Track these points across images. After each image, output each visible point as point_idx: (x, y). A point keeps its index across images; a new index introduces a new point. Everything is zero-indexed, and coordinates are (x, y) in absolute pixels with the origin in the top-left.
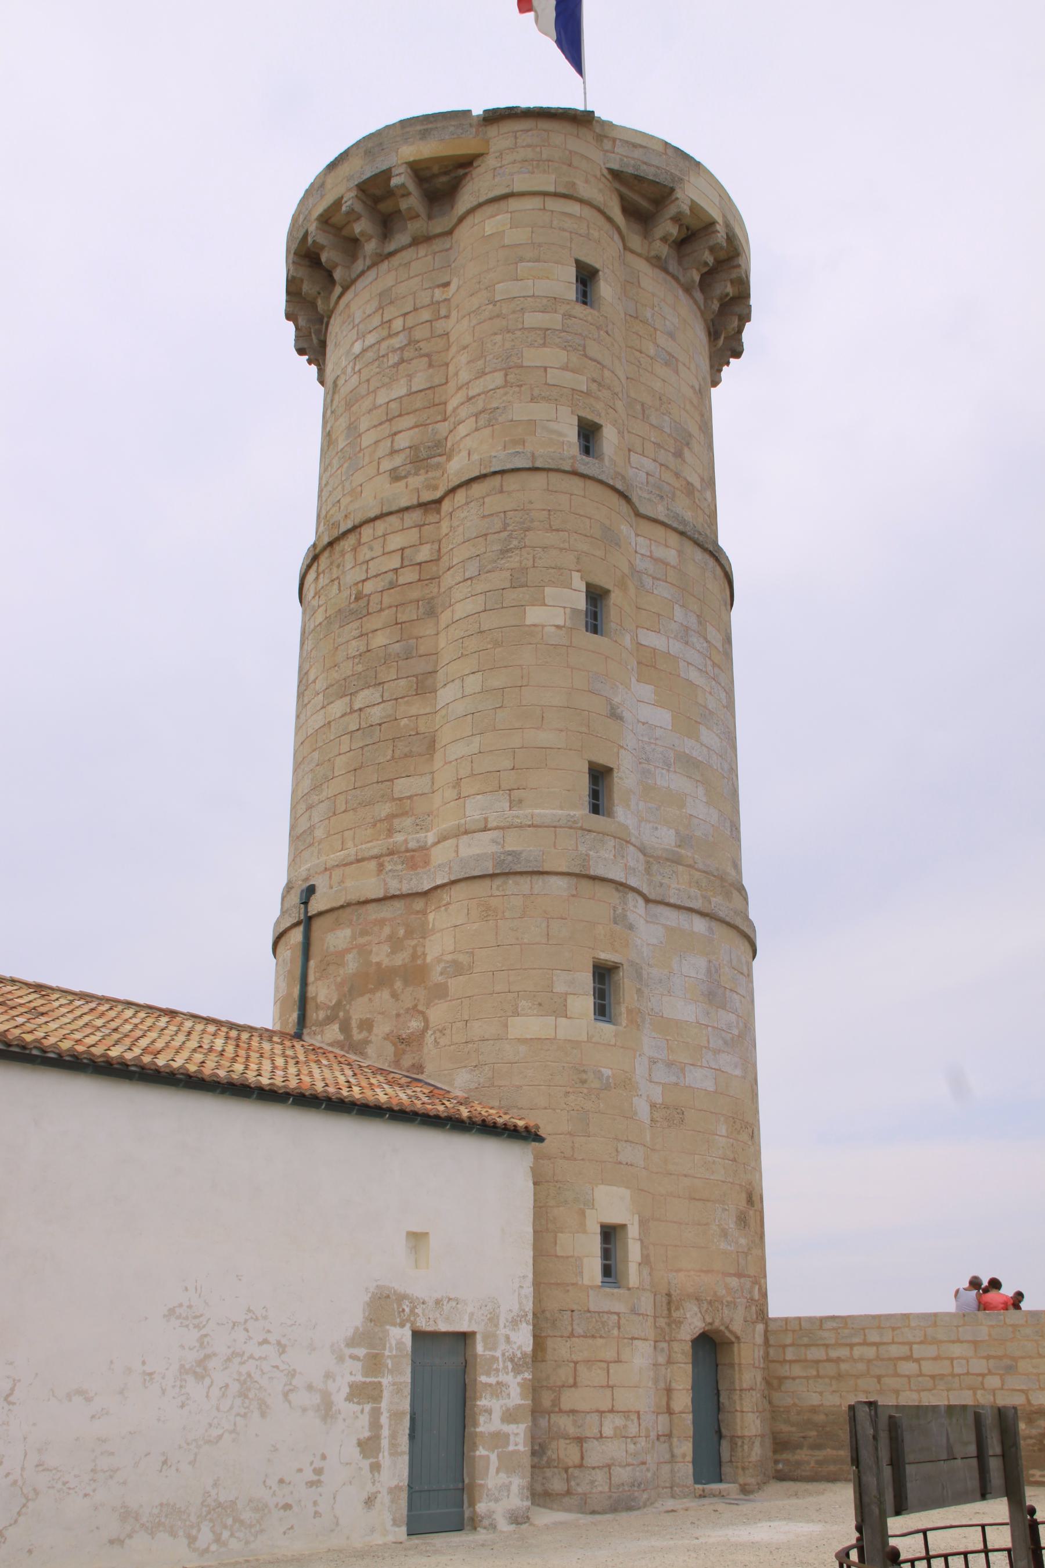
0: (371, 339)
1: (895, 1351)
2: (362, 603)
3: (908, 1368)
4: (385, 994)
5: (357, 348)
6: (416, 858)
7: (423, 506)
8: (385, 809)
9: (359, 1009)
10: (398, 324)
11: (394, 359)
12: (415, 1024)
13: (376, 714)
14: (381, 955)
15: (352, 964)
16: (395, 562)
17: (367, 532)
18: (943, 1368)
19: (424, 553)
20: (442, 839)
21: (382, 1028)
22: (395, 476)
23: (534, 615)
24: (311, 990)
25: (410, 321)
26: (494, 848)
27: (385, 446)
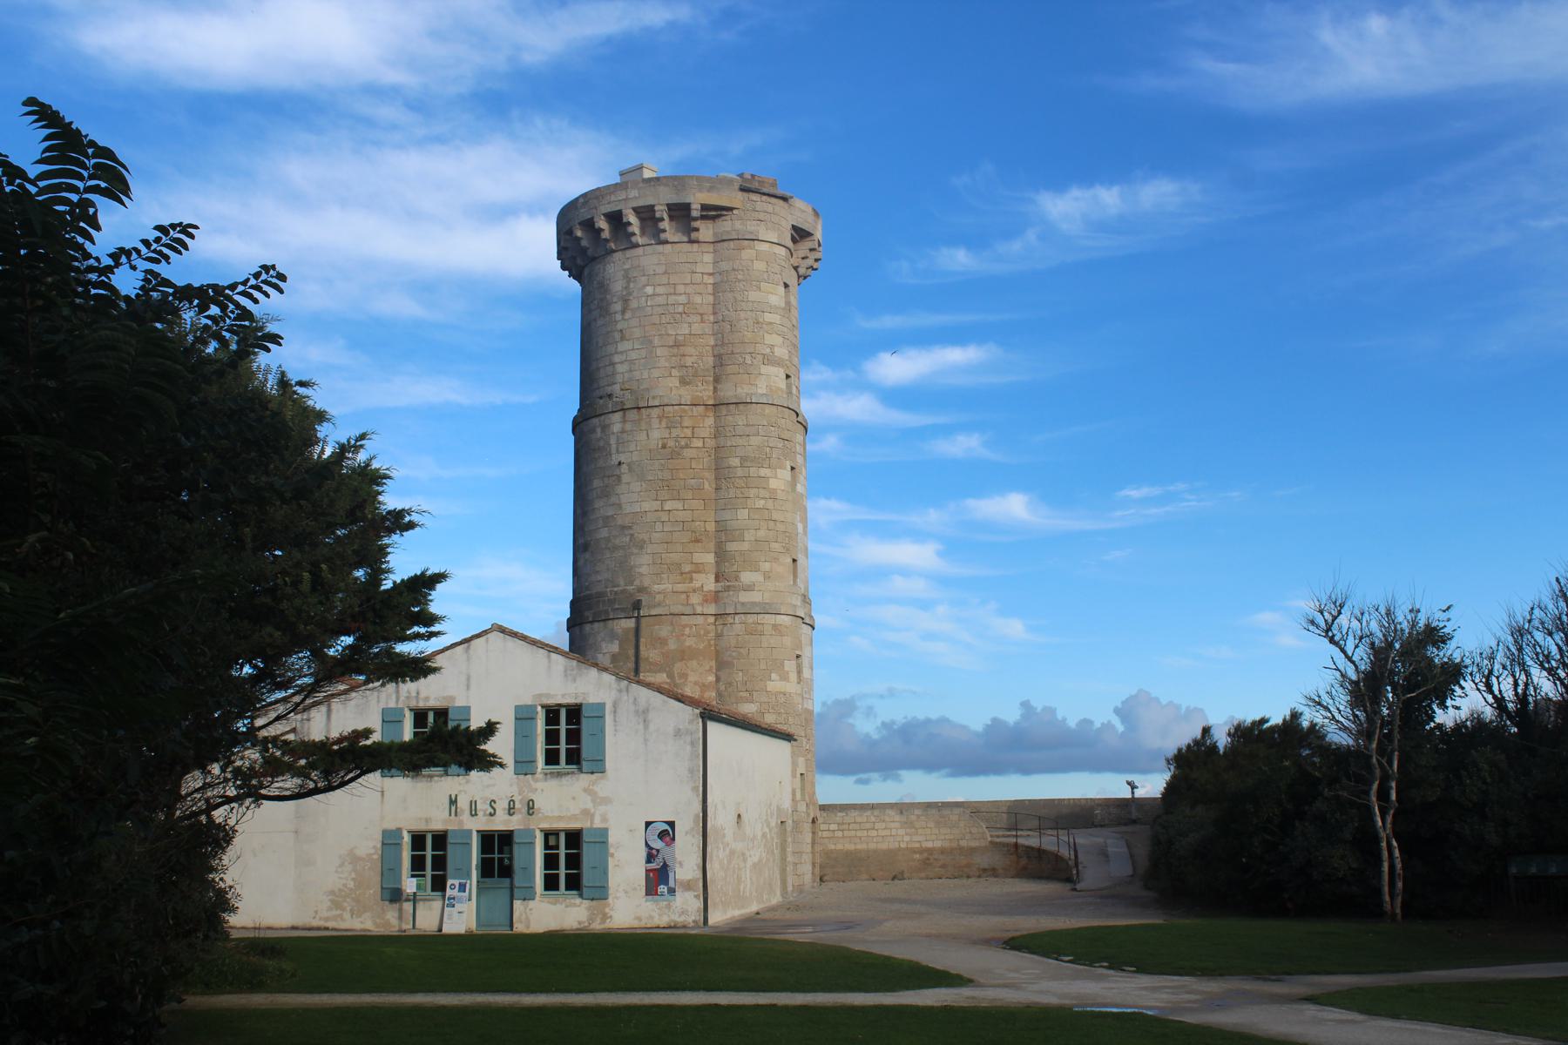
1: (868, 826)
2: (668, 451)
3: (874, 833)
4: (694, 663)
5: (649, 290)
8: (687, 568)
9: (678, 667)
10: (681, 289)
13: (681, 515)
18: (887, 832)
21: (692, 678)
23: (773, 484)
25: (689, 290)
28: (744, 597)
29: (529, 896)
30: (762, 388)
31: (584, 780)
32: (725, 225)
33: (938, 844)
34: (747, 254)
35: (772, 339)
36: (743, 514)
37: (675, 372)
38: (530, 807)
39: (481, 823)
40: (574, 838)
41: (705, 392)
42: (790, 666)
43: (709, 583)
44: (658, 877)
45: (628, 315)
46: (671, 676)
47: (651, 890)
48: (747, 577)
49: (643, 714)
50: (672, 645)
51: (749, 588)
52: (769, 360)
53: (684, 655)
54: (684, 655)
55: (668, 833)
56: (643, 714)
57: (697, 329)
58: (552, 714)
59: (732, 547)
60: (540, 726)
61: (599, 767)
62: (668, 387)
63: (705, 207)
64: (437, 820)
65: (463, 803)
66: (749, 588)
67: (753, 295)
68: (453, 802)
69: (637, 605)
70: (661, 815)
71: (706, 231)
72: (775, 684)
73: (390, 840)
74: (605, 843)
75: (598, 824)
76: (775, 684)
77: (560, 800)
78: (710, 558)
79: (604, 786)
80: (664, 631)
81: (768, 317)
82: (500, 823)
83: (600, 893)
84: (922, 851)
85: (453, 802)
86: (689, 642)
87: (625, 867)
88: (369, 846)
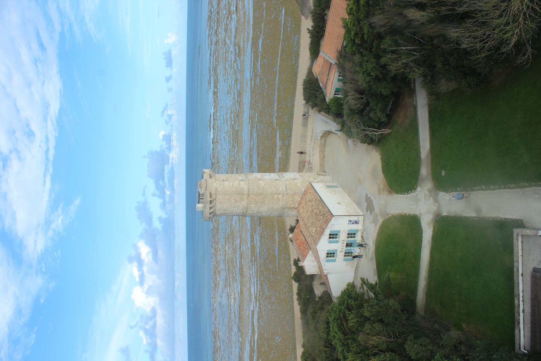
23: (263, 184)
28: (284, 190)
29: (356, 240)
30: (245, 187)
31: (341, 233)
32: (213, 193)
34: (219, 189)
35: (235, 184)
36: (269, 190)
38: (343, 241)
39: (345, 248)
40: (348, 234)
41: (245, 197)
42: (296, 181)
43: (281, 196)
44: (356, 222)
47: (358, 223)
48: (280, 190)
49: (332, 225)
50: (291, 202)
51: (282, 189)
52: (240, 185)
53: (293, 200)
54: (293, 200)
55: (350, 221)
56: (332, 225)
57: (233, 198)
58: (330, 238)
59: (275, 192)
60: (331, 239)
61: (339, 231)
62: (244, 203)
63: (211, 197)
66: (282, 189)
67: (227, 188)
69: (283, 208)
70: (348, 222)
71: (214, 197)
72: (299, 185)
73: (345, 260)
76: (299, 185)
77: (343, 237)
78: (276, 196)
80: (289, 204)
81: (231, 185)
82: (345, 245)
83: (357, 231)
86: (291, 199)
87: (354, 227)
88: (345, 263)
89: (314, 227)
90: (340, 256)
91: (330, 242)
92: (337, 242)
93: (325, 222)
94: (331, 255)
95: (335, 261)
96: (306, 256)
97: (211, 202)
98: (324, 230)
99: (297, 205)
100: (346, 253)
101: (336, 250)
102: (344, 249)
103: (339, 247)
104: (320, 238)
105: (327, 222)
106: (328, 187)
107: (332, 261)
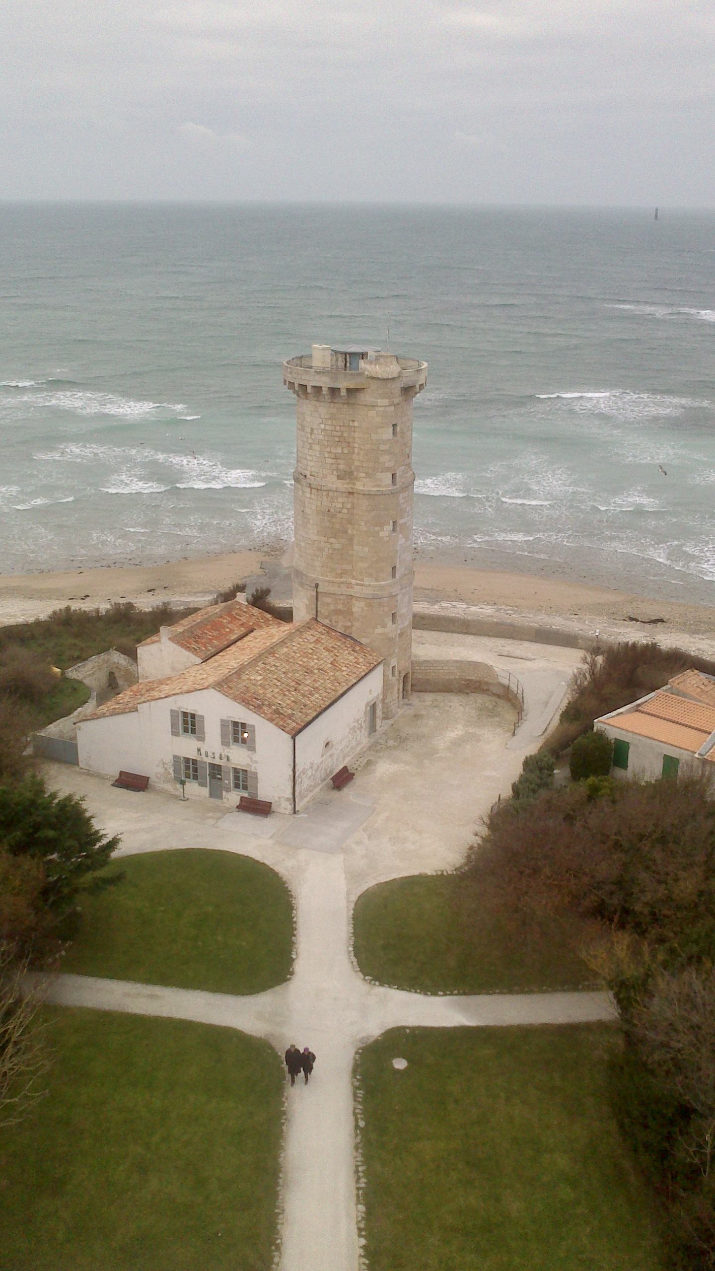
0: (328, 427)
5: (322, 426)
6: (350, 586)
7: (350, 493)
11: (337, 439)
12: (349, 624)
13: (337, 546)
14: (340, 607)
15: (332, 607)
16: (340, 505)
17: (331, 494)
19: (349, 506)
20: (357, 584)
22: (339, 477)
23: (381, 534)
24: (319, 609)
25: (342, 429)
26: (371, 592)
27: (334, 466)
33: (474, 678)
37: (335, 473)
38: (228, 759)
45: (313, 437)
46: (331, 621)
60: (231, 728)
64: (193, 755)
65: (203, 751)
68: (199, 750)
74: (257, 778)
75: (253, 770)
77: (238, 757)
79: (255, 757)
82: (217, 761)
84: (466, 680)
85: (199, 750)
89: (264, 679)
90: (187, 747)
91: (224, 724)
92: (225, 743)
93: (276, 712)
94: (190, 724)
95: (175, 733)
96: (188, 648)
97: (334, 391)
98: (258, 709)
99: (326, 622)
100: (195, 762)
101: (201, 739)
102: (206, 759)
103: (211, 746)
104: (235, 699)
105: (278, 717)
106: (374, 707)
107: (174, 725)
